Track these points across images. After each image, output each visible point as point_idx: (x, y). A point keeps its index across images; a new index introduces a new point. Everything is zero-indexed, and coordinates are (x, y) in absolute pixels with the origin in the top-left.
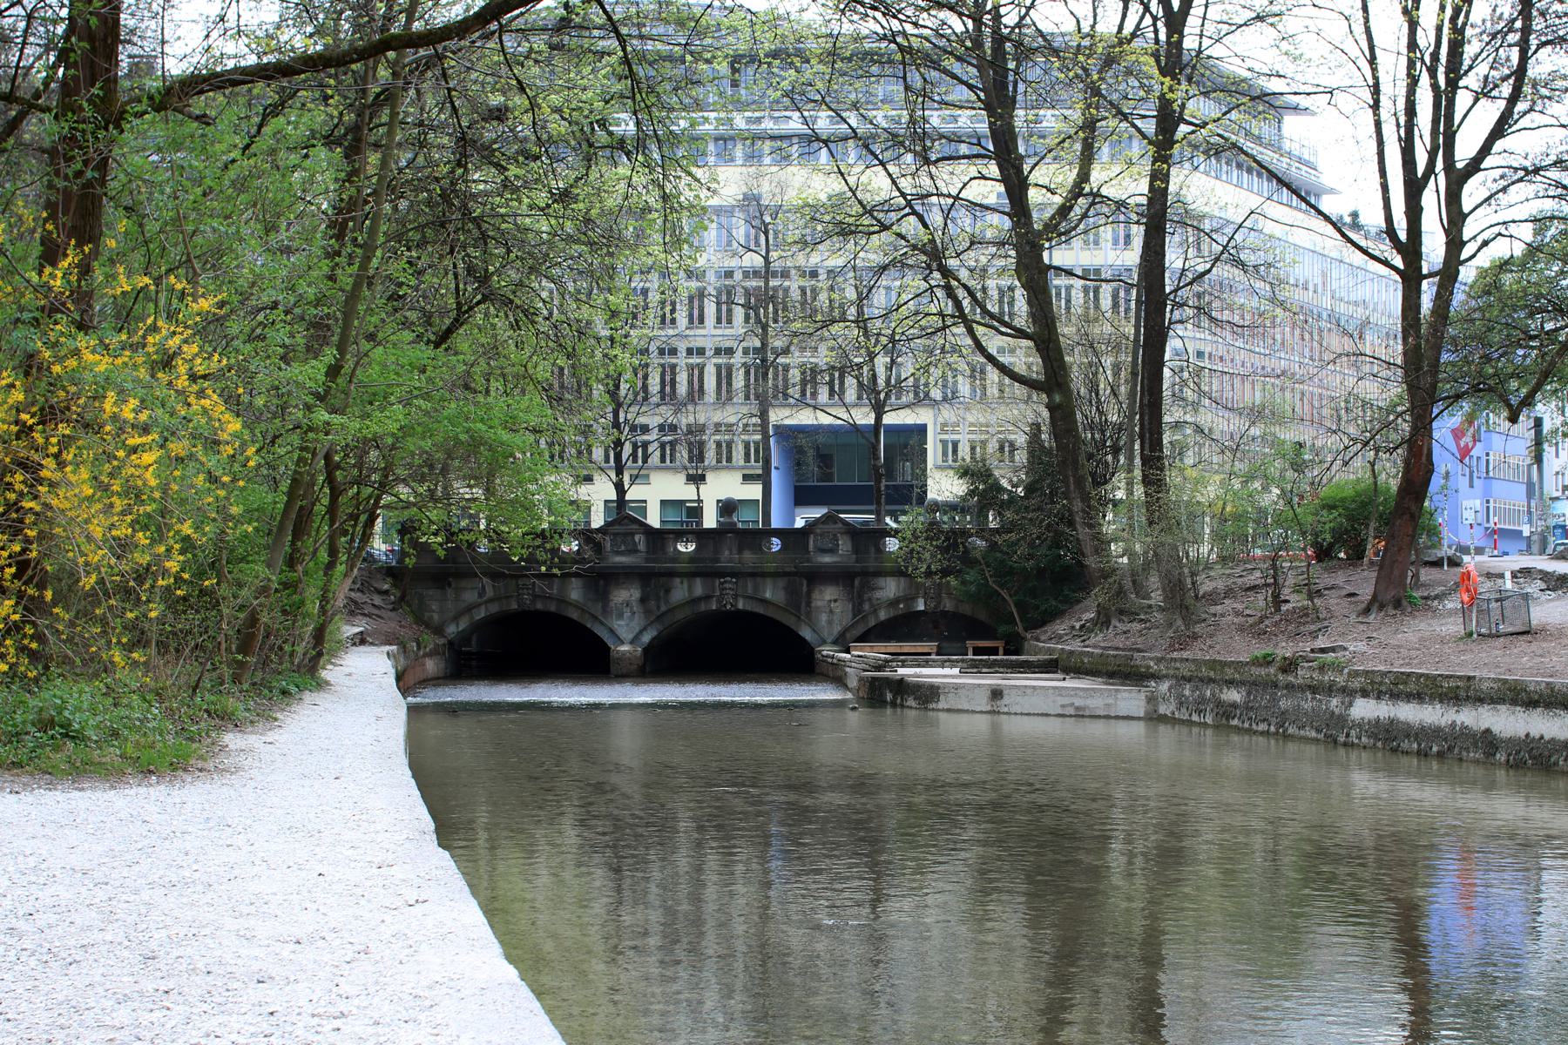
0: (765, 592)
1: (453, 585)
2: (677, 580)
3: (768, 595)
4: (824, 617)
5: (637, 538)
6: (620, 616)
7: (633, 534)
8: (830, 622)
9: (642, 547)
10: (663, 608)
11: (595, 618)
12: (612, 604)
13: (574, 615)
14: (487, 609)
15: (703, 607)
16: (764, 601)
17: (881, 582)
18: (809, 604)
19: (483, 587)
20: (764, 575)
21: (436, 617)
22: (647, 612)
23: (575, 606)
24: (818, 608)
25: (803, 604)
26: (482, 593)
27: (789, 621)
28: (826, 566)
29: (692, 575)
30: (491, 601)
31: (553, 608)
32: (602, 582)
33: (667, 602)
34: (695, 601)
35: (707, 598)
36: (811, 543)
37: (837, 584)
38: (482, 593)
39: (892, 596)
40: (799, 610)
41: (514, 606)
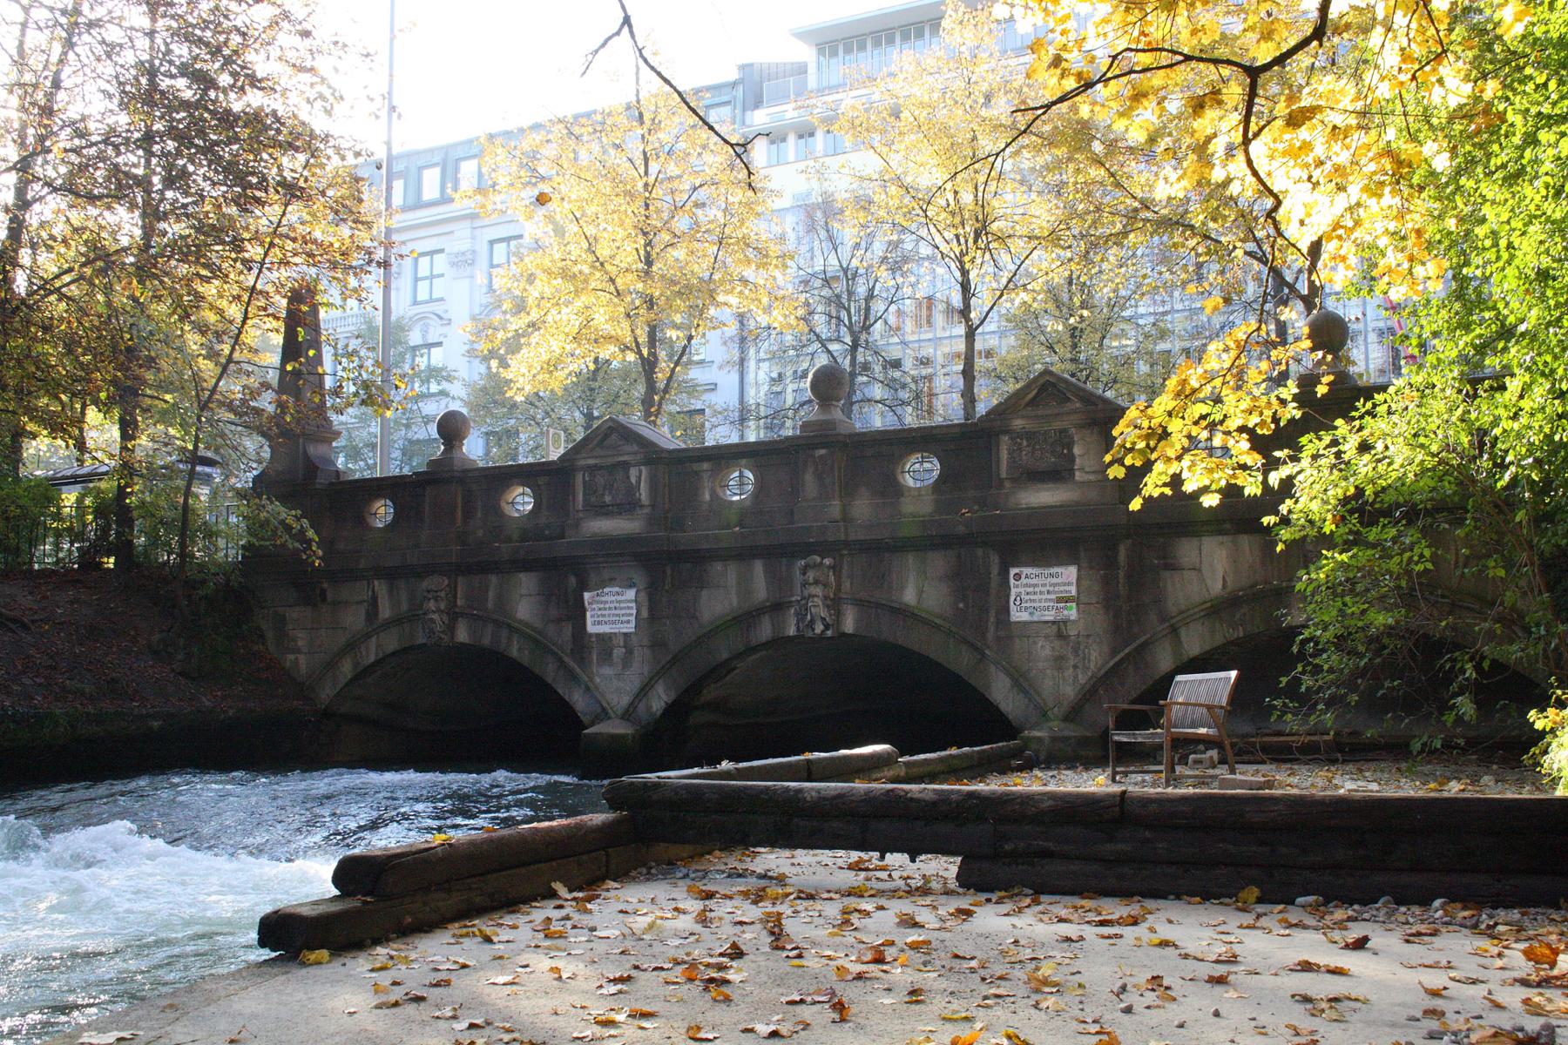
0: (903, 588)
1: (330, 595)
2: (719, 566)
3: (909, 596)
5: (633, 472)
7: (626, 466)
13: (516, 650)
17: (1185, 550)
19: (374, 602)
20: (901, 546)
21: (302, 659)
27: (959, 660)
28: (1047, 511)
29: (743, 554)
30: (387, 625)
34: (745, 619)
35: (777, 608)
39: (1216, 587)
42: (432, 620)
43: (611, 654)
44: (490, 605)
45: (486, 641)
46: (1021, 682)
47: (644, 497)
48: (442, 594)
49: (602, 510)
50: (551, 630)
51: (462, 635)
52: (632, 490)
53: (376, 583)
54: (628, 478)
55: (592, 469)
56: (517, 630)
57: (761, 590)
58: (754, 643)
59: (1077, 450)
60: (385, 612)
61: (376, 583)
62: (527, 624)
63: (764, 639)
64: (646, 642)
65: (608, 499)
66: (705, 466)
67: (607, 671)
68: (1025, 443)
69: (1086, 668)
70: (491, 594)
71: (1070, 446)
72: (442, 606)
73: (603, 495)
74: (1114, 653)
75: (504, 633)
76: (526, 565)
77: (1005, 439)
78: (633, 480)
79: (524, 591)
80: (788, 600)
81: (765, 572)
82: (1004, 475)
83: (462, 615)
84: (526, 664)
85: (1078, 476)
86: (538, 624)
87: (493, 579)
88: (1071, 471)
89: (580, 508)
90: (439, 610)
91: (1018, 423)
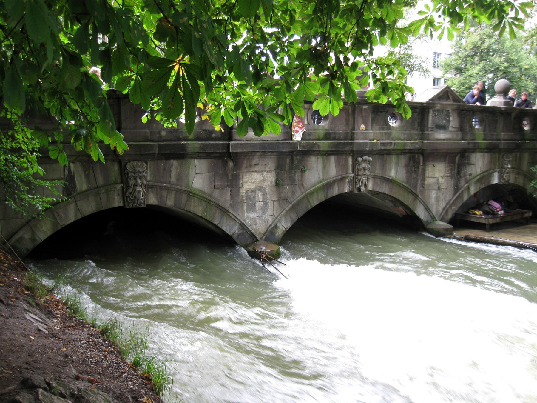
0: (390, 170)
4: (433, 194)
6: (252, 207)
8: (437, 199)
11: (224, 211)
12: (243, 191)
14: (78, 209)
15: (335, 191)
16: (389, 181)
18: (424, 179)
22: (282, 200)
24: (429, 185)
25: (419, 182)
27: (407, 199)
30: (84, 194)
31: (170, 202)
32: (231, 164)
34: (329, 186)
37: (445, 161)
40: (416, 188)
41: (117, 202)
43: (254, 206)
44: (173, 180)
46: (427, 209)
50: (216, 194)
56: (194, 195)
57: (333, 171)
59: (451, 119)
62: (200, 191)
64: (275, 198)
67: (253, 215)
69: (445, 200)
70: (173, 173)
71: (449, 116)
74: (455, 194)
75: (184, 197)
76: (199, 155)
77: (431, 111)
79: (198, 171)
81: (335, 162)
82: (430, 125)
85: (450, 129)
86: (207, 190)
87: (175, 163)
88: (448, 127)
91: (438, 107)
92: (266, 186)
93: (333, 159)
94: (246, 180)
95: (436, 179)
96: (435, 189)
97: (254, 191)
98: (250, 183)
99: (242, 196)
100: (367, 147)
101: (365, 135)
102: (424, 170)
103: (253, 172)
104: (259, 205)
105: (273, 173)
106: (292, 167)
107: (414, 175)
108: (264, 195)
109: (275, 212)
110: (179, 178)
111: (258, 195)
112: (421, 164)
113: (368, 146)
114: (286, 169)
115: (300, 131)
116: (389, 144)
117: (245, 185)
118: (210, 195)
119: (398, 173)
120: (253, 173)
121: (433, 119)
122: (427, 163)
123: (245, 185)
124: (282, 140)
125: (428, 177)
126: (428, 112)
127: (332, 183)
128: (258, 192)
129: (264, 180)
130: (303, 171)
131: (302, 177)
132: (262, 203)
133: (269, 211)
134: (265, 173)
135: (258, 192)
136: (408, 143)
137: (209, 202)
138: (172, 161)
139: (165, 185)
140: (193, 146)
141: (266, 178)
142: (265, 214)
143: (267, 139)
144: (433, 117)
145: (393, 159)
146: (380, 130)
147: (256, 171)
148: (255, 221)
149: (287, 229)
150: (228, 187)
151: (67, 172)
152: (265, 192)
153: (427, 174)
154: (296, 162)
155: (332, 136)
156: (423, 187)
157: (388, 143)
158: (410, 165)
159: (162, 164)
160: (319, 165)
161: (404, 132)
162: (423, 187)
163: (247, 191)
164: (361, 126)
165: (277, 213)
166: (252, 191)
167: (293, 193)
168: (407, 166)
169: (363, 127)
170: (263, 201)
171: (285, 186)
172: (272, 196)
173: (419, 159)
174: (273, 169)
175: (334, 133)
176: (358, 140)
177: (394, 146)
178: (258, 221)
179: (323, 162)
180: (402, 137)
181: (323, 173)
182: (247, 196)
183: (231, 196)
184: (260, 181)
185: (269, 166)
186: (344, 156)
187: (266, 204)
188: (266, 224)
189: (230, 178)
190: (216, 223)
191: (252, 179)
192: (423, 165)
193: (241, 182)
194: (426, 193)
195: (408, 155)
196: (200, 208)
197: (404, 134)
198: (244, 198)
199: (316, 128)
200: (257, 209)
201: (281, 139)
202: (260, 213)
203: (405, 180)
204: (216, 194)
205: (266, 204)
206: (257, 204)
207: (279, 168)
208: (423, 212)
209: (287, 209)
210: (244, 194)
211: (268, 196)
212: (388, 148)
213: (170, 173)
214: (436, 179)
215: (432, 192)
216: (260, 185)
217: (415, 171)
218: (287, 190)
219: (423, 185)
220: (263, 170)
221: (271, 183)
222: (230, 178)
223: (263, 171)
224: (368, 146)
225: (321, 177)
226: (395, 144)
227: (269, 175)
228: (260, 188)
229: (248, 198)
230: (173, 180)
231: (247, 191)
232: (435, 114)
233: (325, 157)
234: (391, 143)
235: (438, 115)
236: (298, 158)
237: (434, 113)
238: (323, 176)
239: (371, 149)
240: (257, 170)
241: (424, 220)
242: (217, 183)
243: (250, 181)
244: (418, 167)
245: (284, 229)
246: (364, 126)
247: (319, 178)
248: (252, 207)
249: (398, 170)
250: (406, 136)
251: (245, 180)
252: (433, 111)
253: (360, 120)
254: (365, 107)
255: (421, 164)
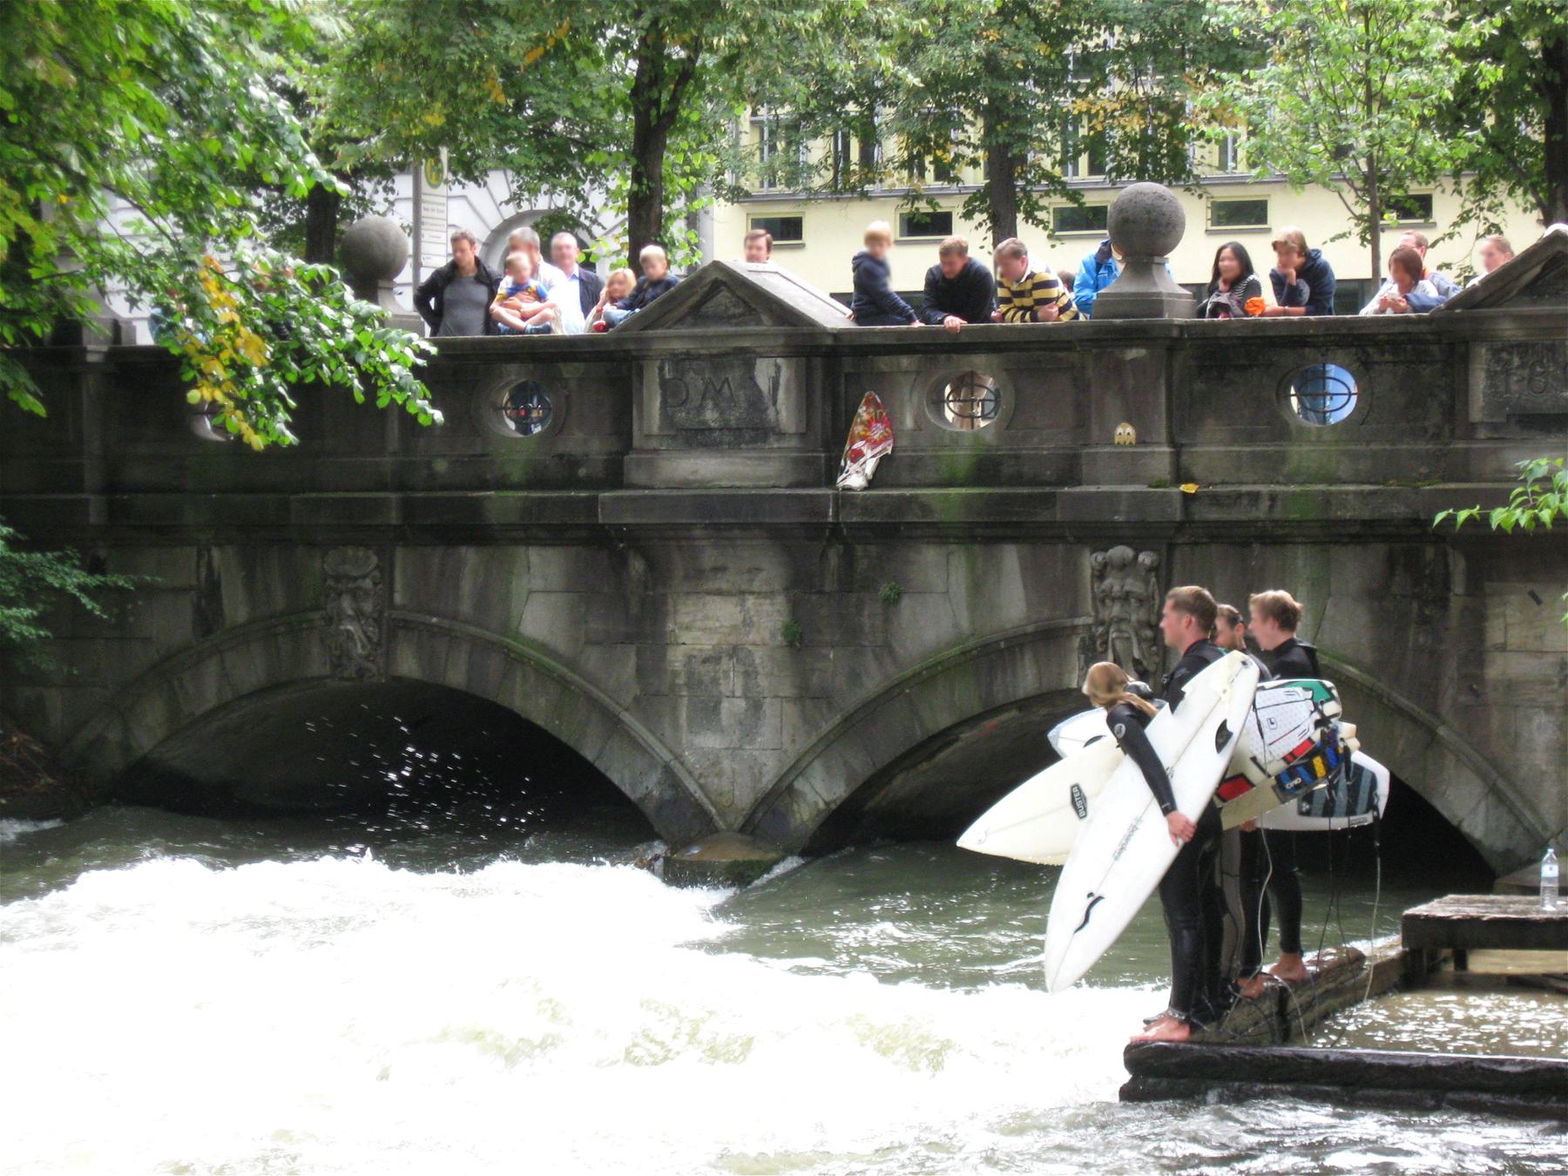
2: (930, 555)
5: (764, 371)
6: (708, 712)
7: (746, 358)
9: (784, 412)
10: (873, 683)
12: (676, 658)
18: (1477, 654)
19: (212, 591)
22: (809, 696)
23: (543, 672)
24: (1511, 686)
25: (1451, 669)
26: (208, 617)
32: (637, 566)
33: (886, 648)
36: (1479, 382)
38: (208, 617)
42: (349, 635)
44: (466, 607)
45: (456, 677)
47: (784, 415)
48: (368, 583)
49: (696, 438)
50: (592, 659)
51: (408, 665)
52: (756, 402)
53: (215, 553)
54: (752, 378)
55: (681, 361)
56: (521, 660)
58: (1000, 698)
60: (236, 608)
61: (215, 553)
62: (543, 647)
63: (1021, 694)
64: (787, 690)
65: (710, 416)
66: (905, 361)
67: (710, 741)
68: (1516, 361)
70: (466, 587)
72: (368, 607)
73: (701, 409)
77: (1482, 353)
78: (763, 383)
80: (1068, 622)
83: (407, 625)
84: (540, 722)
86: (561, 644)
87: (470, 556)
89: (655, 429)
90: (359, 615)
91: (1508, 330)
92: (754, 644)
93: (1011, 558)
94: (686, 620)
95: (1550, 659)
96: (1548, 709)
97: (713, 659)
98: (704, 630)
99: (675, 674)
100: (1116, 513)
101: (1129, 464)
102: (1477, 620)
103: (709, 593)
104: (733, 708)
105: (780, 599)
106: (851, 583)
107: (1417, 637)
108: (747, 674)
109: (786, 738)
110: (482, 599)
111: (726, 673)
112: (1458, 587)
113: (1123, 507)
114: (827, 589)
115: (868, 453)
116: (1245, 501)
117: (685, 637)
118: (571, 664)
119: (1326, 625)
120: (708, 598)
121: (1492, 386)
122: (1489, 586)
123: (685, 637)
124: (789, 486)
125: (1503, 648)
126: (1465, 361)
127: (1010, 649)
128: (726, 664)
129: (748, 623)
130: (892, 602)
131: (887, 620)
132: (742, 704)
133: (767, 734)
134: (750, 601)
135: (726, 664)
136: (1347, 493)
137: (563, 683)
138: (463, 550)
139: (434, 620)
140: (501, 504)
141: (755, 619)
142: (752, 742)
143: (737, 484)
144: (1491, 375)
145: (1300, 563)
146: (1234, 441)
147: (719, 593)
148: (716, 763)
149: (833, 806)
150: (628, 639)
151: (204, 571)
152: (752, 664)
153: (1495, 634)
154: (862, 565)
155: (1007, 470)
156: (1476, 694)
157: (1239, 496)
158: (1395, 589)
159: (436, 556)
160: (953, 579)
161: (1362, 447)
162: (1476, 694)
163: (690, 658)
164: (1119, 430)
165: (794, 741)
166: (705, 661)
167: (855, 677)
168: (1376, 595)
169: (1125, 432)
170: (745, 696)
171: (824, 651)
172: (774, 682)
173: (1446, 566)
174: (777, 586)
175: (1017, 457)
176: (1096, 482)
177: (1271, 507)
178: (726, 764)
179: (972, 569)
180: (1344, 469)
181: (973, 608)
182: (691, 674)
183: (640, 671)
184: (735, 627)
185: (763, 575)
186: (1061, 547)
187: (756, 706)
188: (756, 779)
189: (635, 609)
190: (589, 754)
191: (706, 617)
192: (1468, 594)
193: (670, 626)
194: (1495, 723)
195: (1381, 549)
196: (542, 701)
197: (1354, 457)
198: (681, 681)
199: (947, 441)
200: (725, 722)
201: (785, 482)
202: (735, 738)
203: (1368, 657)
204: (592, 659)
205: (756, 706)
206: (725, 705)
207: (800, 586)
208: (1482, 808)
209: (825, 728)
210: (678, 666)
211: (763, 682)
212: (1243, 517)
213: (457, 587)
214: (1550, 659)
215: (1529, 719)
216: (732, 640)
217: (1424, 621)
218: (831, 662)
219: (1473, 682)
220: (744, 587)
221: (773, 635)
222: (635, 609)
223: (742, 593)
224: (1123, 507)
225: (965, 623)
226: (1273, 497)
227: (767, 606)
228: (734, 651)
229: (694, 682)
230: (466, 607)
231: (690, 658)
232: (1508, 363)
233: (976, 548)
234: (1255, 497)
235: (1522, 366)
236: (873, 549)
237: (1498, 361)
238: (972, 623)
239: (1134, 517)
240: (724, 586)
241: (1487, 842)
242: (596, 626)
243: (698, 624)
244: (1443, 602)
245: (822, 805)
246: (1129, 429)
247: (956, 625)
248: (708, 712)
249: (1330, 612)
250: (1364, 466)
251: (684, 619)
252: (1495, 352)
253: (1113, 404)
254: (1133, 353)
255: (1458, 587)
